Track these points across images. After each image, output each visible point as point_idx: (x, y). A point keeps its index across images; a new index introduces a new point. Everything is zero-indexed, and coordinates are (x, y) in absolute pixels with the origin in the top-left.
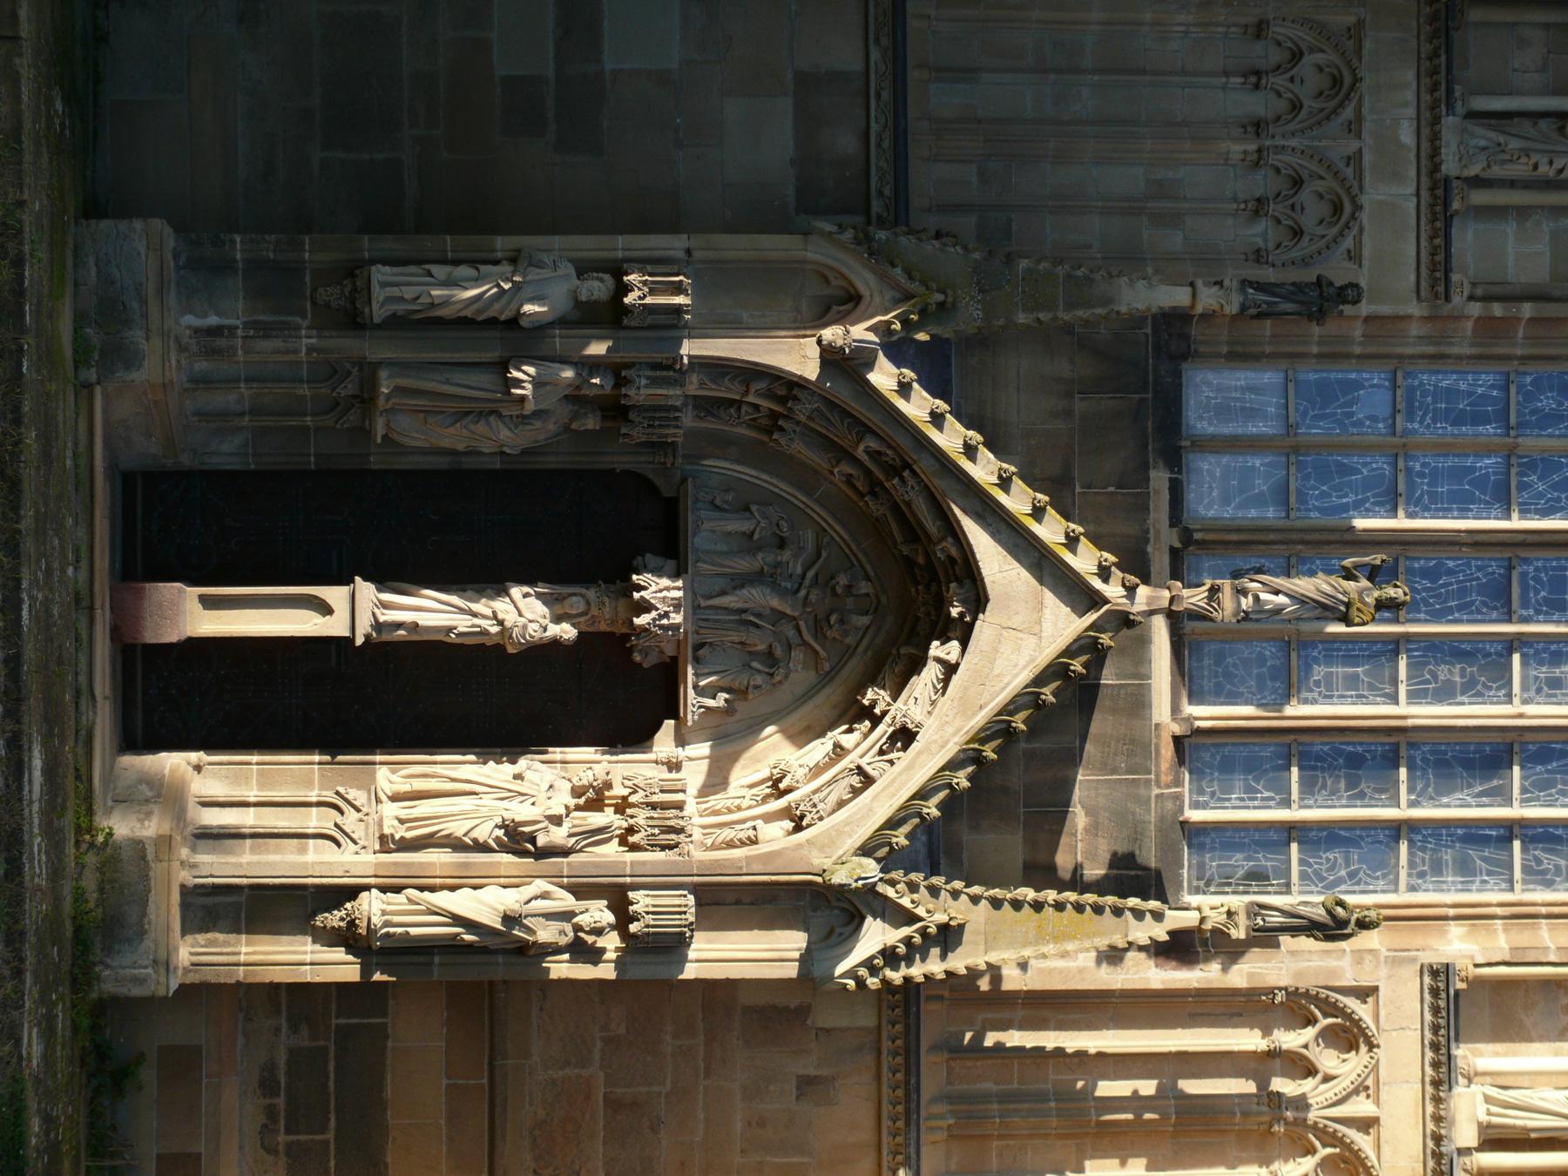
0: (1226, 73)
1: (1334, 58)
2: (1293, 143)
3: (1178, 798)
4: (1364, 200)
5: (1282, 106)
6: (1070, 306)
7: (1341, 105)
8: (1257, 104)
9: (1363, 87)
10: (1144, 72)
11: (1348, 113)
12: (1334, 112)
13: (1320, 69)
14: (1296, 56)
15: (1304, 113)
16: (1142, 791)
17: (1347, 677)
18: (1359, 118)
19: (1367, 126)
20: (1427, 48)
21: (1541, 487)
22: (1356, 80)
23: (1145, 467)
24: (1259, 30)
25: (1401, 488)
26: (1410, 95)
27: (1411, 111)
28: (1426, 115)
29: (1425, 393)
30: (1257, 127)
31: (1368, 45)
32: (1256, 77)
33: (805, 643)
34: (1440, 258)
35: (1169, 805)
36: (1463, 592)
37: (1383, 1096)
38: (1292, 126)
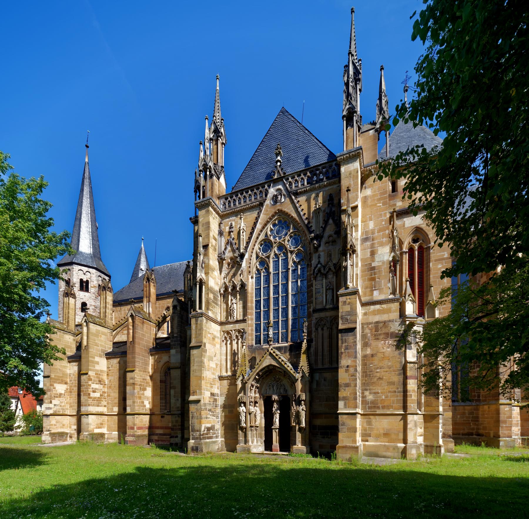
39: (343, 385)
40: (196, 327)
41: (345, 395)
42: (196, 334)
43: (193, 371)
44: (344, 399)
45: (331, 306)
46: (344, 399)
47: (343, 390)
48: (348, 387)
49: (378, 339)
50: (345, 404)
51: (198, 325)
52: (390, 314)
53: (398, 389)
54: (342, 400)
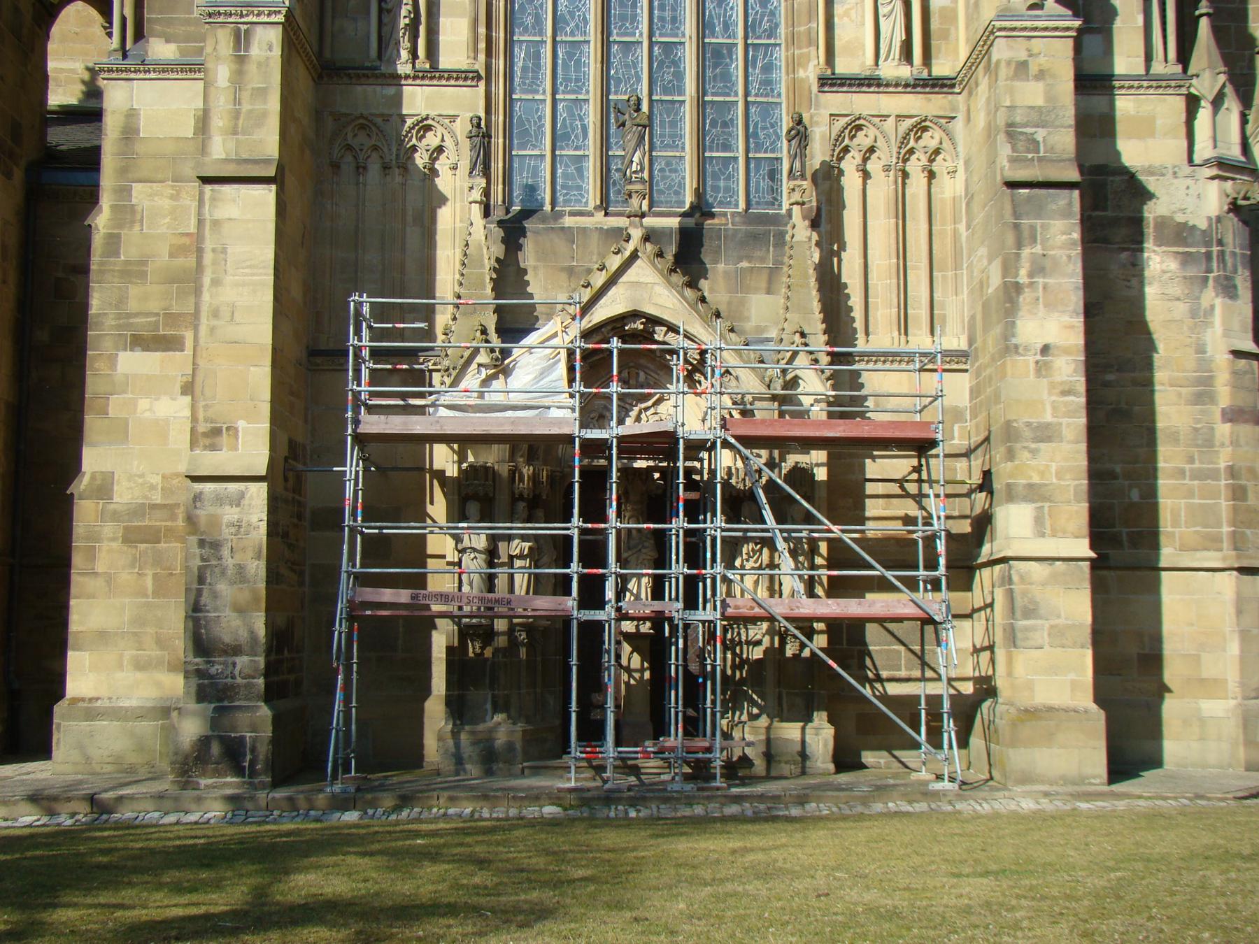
0: (358, 184)
1: (350, 128)
2: (394, 150)
3: (733, 214)
4: (424, 114)
5: (375, 155)
6: (482, 266)
7: (375, 125)
8: (374, 168)
9: (365, 113)
10: (357, 227)
11: (379, 121)
12: (378, 128)
13: (355, 136)
14: (349, 148)
15: (379, 144)
16: (730, 233)
17: (670, 127)
18: (382, 115)
19: (386, 111)
20: (346, 80)
21: (572, 25)
22: (362, 116)
23: (563, 229)
24: (336, 166)
25: (573, 97)
26: (370, 89)
27: (378, 88)
28: (380, 81)
29: (524, 84)
30: (386, 168)
31: (343, 110)
32: (361, 169)
33: (654, 405)
34: (455, 75)
35: (737, 219)
36: (627, 66)
37: (885, 113)
38: (386, 150)
39: (1027, 433)
40: (238, 77)
41: (1036, 479)
42: (236, 115)
43: (215, 314)
44: (1034, 493)
45: (905, 72)
46: (1034, 493)
47: (1026, 454)
48: (1048, 439)
49: (1106, 241)
50: (1039, 520)
51: (252, 68)
52: (1150, 142)
53: (1191, 460)
54: (1026, 499)
